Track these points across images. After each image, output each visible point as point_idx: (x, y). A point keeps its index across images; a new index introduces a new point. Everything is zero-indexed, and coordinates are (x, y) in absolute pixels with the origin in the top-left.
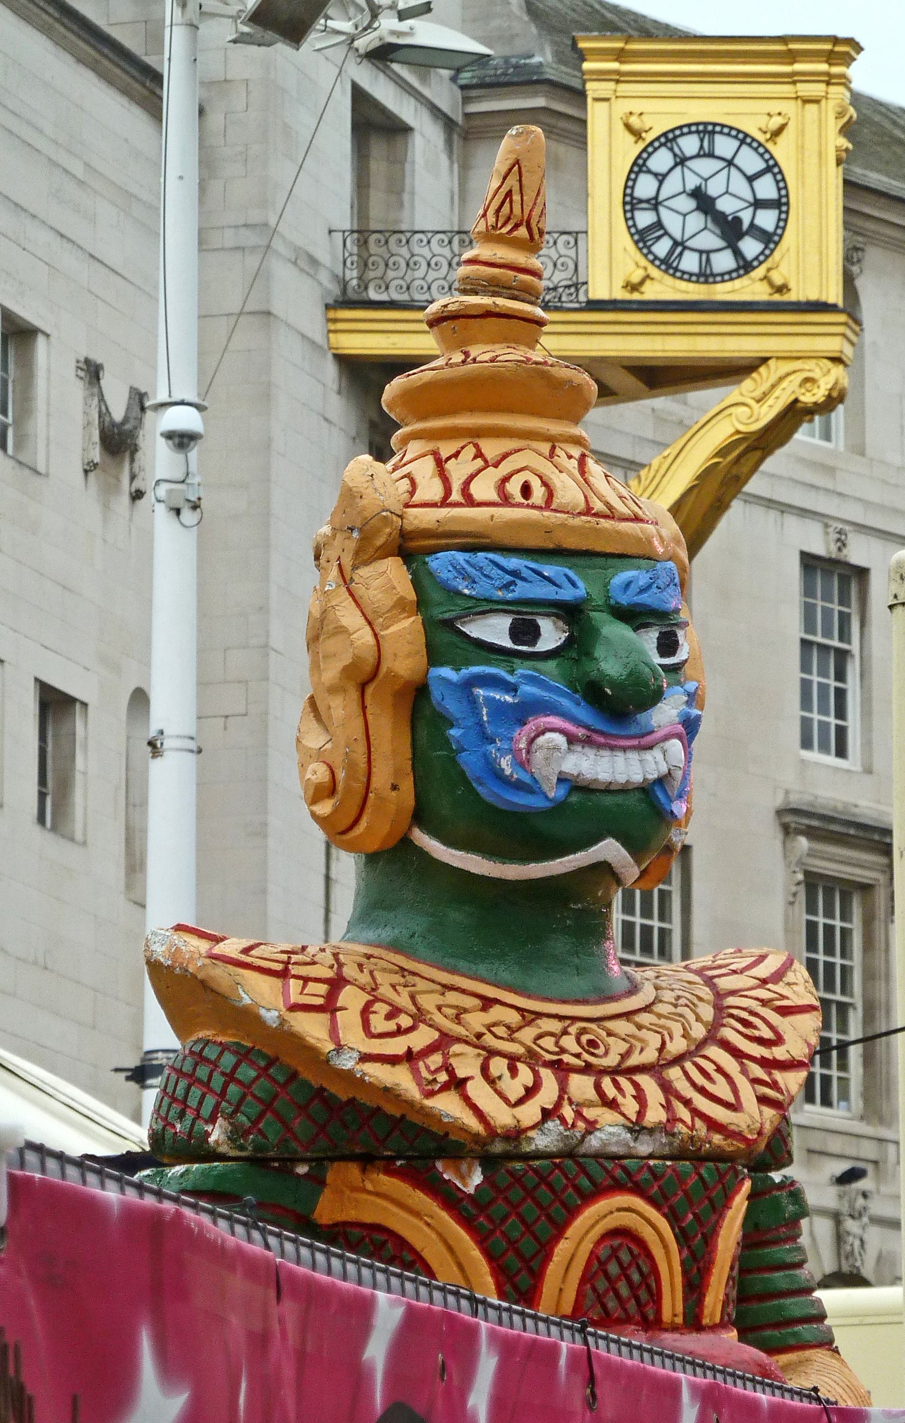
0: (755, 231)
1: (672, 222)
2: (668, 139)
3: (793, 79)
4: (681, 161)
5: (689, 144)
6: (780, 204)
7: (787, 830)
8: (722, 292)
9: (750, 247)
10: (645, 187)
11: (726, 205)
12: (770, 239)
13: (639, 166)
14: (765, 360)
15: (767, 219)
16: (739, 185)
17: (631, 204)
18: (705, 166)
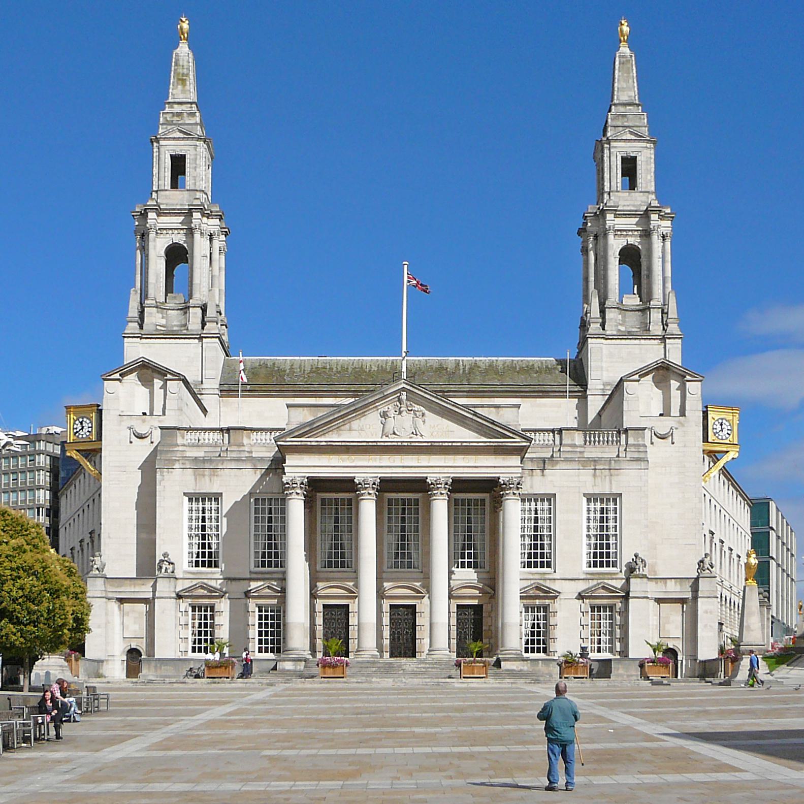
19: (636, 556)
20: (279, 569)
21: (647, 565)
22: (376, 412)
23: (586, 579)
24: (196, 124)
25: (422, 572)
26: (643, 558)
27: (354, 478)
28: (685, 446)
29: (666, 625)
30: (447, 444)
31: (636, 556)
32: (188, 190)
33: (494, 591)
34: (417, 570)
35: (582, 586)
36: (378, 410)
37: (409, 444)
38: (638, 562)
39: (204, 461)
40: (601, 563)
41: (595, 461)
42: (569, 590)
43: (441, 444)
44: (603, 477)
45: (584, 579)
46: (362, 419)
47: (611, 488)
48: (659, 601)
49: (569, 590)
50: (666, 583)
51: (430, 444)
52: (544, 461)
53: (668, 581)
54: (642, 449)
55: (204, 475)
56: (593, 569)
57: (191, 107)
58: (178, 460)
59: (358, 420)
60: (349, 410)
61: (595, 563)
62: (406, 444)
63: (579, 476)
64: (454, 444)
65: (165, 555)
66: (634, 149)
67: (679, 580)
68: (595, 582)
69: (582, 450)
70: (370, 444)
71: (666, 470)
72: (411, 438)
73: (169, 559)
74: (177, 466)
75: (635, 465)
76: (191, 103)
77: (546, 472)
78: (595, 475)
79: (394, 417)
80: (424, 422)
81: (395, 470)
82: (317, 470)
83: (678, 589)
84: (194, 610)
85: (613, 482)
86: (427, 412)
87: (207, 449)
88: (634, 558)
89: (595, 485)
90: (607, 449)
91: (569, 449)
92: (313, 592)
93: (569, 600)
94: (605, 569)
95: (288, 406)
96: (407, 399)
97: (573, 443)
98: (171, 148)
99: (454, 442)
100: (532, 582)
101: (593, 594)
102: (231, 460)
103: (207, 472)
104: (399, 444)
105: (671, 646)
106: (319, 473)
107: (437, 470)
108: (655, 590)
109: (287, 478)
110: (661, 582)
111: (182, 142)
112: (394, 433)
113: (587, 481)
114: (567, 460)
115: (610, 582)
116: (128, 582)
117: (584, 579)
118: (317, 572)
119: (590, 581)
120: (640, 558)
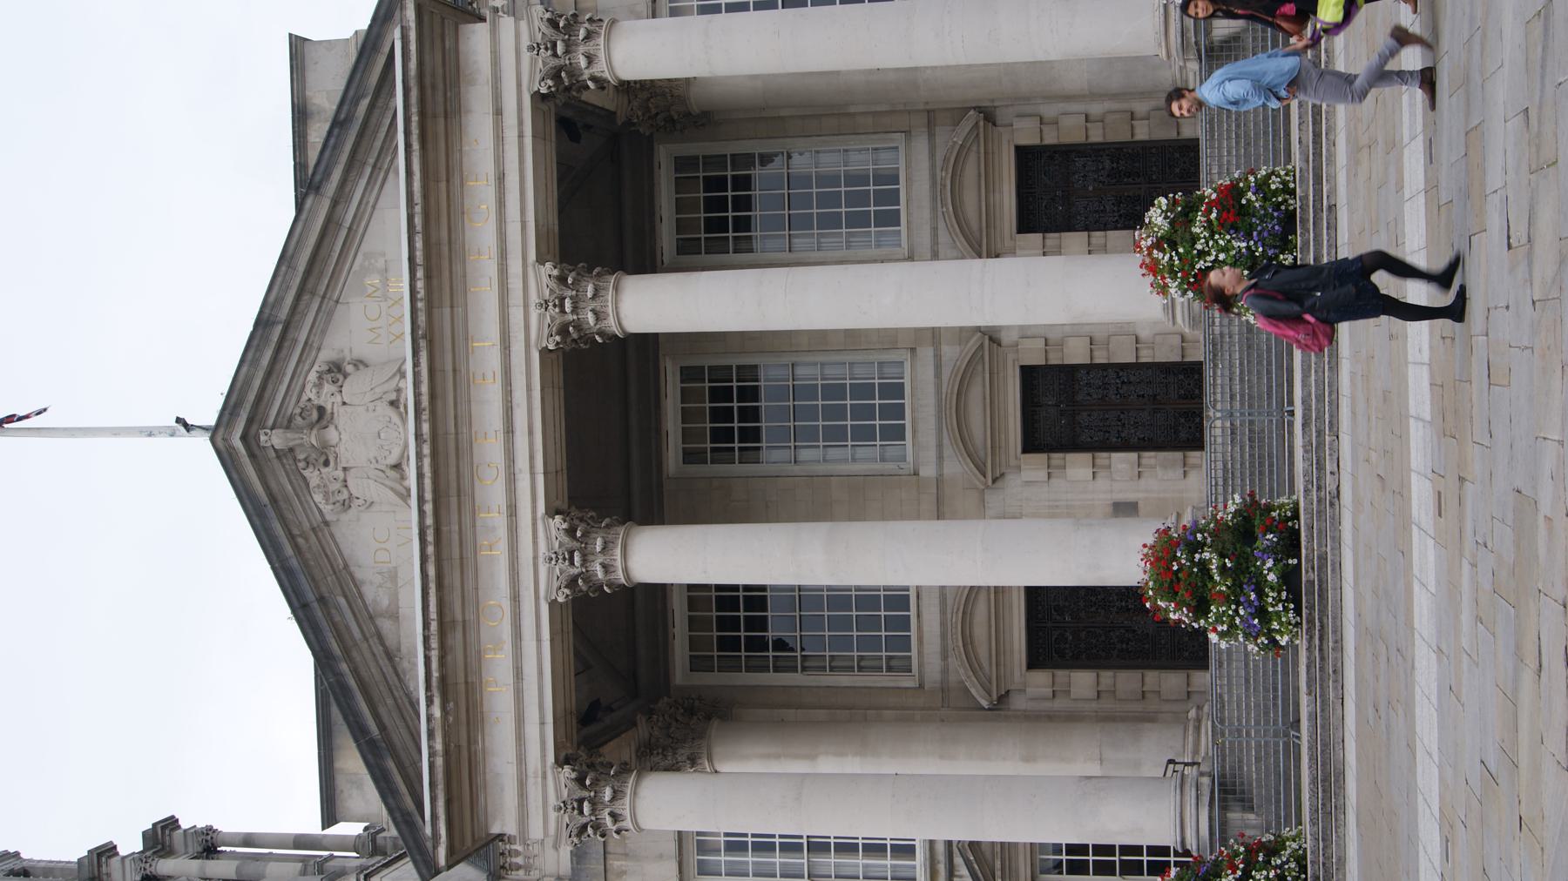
22: (334, 529)
25: (913, 350)
27: (553, 604)
30: (420, 285)
33: (969, 109)
34: (907, 365)
36: (327, 523)
37: (425, 416)
43: (420, 305)
46: (359, 575)
51: (423, 344)
62: (426, 427)
64: (419, 254)
70: (430, 549)
72: (406, 412)
79: (345, 469)
80: (359, 363)
82: (532, 731)
86: (326, 355)
92: (985, 703)
96: (288, 428)
99: (411, 259)
104: (426, 450)
106: (542, 723)
112: (397, 467)
118: (921, 686)
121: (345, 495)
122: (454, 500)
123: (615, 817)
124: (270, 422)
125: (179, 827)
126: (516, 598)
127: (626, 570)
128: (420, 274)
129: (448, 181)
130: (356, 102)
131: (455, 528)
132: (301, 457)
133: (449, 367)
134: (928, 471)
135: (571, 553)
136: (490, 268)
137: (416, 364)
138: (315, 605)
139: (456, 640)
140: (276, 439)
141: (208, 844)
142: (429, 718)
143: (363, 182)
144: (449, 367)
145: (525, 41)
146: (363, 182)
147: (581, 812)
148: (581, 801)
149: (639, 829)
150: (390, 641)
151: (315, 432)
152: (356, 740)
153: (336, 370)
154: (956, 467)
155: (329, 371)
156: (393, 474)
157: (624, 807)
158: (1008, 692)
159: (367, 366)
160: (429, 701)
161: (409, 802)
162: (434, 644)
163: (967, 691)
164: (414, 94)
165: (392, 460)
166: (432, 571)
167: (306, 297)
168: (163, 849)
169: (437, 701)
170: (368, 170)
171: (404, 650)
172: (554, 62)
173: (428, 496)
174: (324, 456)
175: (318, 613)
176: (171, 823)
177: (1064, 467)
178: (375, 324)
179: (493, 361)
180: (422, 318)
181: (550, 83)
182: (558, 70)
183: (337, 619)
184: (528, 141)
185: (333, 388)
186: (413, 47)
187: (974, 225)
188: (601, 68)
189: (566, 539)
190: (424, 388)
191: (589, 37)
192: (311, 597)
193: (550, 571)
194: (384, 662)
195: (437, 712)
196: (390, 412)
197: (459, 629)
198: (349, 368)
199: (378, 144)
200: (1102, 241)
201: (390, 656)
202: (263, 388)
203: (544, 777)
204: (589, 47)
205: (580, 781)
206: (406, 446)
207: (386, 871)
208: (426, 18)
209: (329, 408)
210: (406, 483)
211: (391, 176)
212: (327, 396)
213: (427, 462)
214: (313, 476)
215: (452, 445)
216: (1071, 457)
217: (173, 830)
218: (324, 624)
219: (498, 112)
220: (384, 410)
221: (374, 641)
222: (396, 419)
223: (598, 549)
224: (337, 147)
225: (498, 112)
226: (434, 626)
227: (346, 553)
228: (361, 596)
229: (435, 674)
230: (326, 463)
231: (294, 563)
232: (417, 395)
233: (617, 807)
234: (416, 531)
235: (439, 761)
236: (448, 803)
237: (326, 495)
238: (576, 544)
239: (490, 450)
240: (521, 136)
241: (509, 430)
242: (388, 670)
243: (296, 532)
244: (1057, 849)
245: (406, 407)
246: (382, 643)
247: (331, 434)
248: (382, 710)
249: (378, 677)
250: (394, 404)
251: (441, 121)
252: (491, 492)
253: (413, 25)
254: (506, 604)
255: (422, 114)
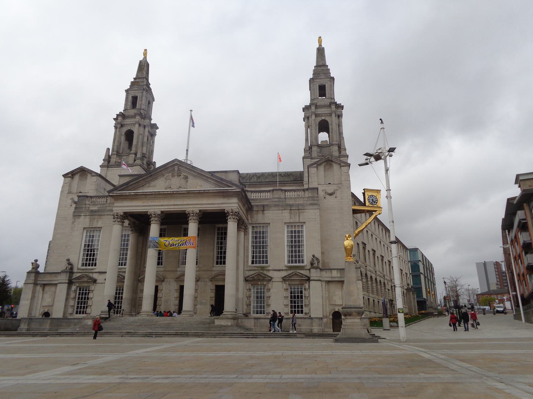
0: (376, 202)
1: (371, 201)
2: (370, 196)
3: (378, 192)
4: (371, 197)
5: (371, 196)
6: (377, 200)
7: (362, 244)
8: (374, 206)
9: (376, 203)
10: (369, 199)
11: (374, 200)
12: (377, 203)
13: (368, 197)
14: (377, 211)
15: (376, 201)
16: (375, 199)
17: (368, 200)
18: (373, 198)
19: (314, 256)
20: (123, 266)
21: (321, 262)
22: (163, 177)
23: (287, 270)
24: (144, 85)
26: (318, 257)
28: (342, 199)
29: (333, 297)
30: (196, 192)
31: (314, 256)
32: (137, 109)
35: (284, 274)
36: (164, 176)
37: (177, 192)
38: (314, 260)
39: (96, 211)
40: (296, 261)
41: (291, 206)
42: (277, 276)
44: (295, 214)
45: (285, 270)
47: (299, 220)
48: (328, 282)
49: (277, 276)
50: (331, 272)
51: (187, 192)
52: (264, 206)
53: (333, 271)
54: (316, 199)
55: (94, 219)
56: (291, 264)
57: (144, 79)
58: (83, 212)
59: (153, 182)
60: (147, 176)
61: (292, 261)
62: (175, 192)
63: (282, 213)
65: (68, 260)
66: (325, 82)
67: (339, 270)
68: (292, 271)
69: (284, 200)
70: (156, 193)
71: (332, 211)
72: (178, 189)
73: (70, 262)
74: (82, 215)
75: (311, 207)
76: (143, 78)
77: (265, 212)
78: (290, 213)
79: (171, 179)
80: (187, 181)
81: (170, 207)
83: (339, 275)
84: (80, 290)
85: (300, 216)
87: (99, 206)
88: (313, 258)
89: (291, 218)
90: (298, 199)
91: (277, 200)
93: (277, 282)
94: (298, 264)
95: (120, 176)
96: (179, 170)
97: (280, 197)
98: (133, 93)
99: (200, 190)
100: (257, 271)
101: (290, 279)
102: (108, 211)
103: (96, 217)
104: (172, 192)
105: (337, 310)
107: (192, 206)
108: (326, 275)
109: (113, 213)
110: (328, 272)
111: (137, 91)
112: (170, 187)
113: (286, 215)
114: (276, 206)
115: (300, 271)
116: (48, 275)
117: (285, 270)
119: (289, 271)
120: (316, 257)
121: (167, 179)
122: (165, 196)
123: (115, 221)
124: (179, 167)
125: (157, 129)
126: (149, 206)
127: (152, 223)
128: (198, 192)
129: (213, 196)
130: (225, 182)
131: (160, 197)
132: (173, 172)
133: (185, 196)
134: (179, 269)
135: (155, 215)
136: (199, 203)
137: (184, 191)
138: (150, 175)
139: (144, 196)
140: (176, 168)
141: (153, 135)
142: (131, 193)
143: (214, 182)
144: (185, 196)
145: (232, 208)
146: (214, 182)
147: (116, 216)
148: (118, 216)
149: (114, 224)
150: (145, 186)
151: (177, 175)
152: (129, 181)
153: (186, 178)
154: (179, 273)
155: (186, 177)
156: (169, 186)
157: (116, 223)
158: (141, 282)
159: (187, 182)
160: (134, 193)
161: (120, 189)
162: (142, 193)
163: (142, 275)
164: (225, 191)
165: (172, 187)
166: (153, 193)
167: (197, 173)
168: (152, 127)
169: (134, 194)
170: (215, 183)
171: (144, 188)
172: (230, 213)
173: (165, 193)
174: (173, 176)
175: (150, 175)
176: (157, 128)
177: (177, 292)
178: (193, 184)
179: (185, 203)
180: (191, 192)
181: (226, 212)
182: (229, 213)
183: (149, 178)
184: (218, 208)
185: (183, 178)
186: (232, 191)
187: (217, 278)
188: (229, 220)
189: (157, 214)
190: (181, 192)
191: (233, 218)
192: (152, 174)
193: (152, 211)
194: (142, 185)
195: (132, 194)
196: (179, 186)
197: (145, 197)
198: (186, 180)
199: (219, 184)
200: (213, 299)
201: (143, 186)
202: (184, 166)
203: (122, 210)
204: (232, 218)
205: (121, 216)
206: (173, 189)
207: (141, 168)
208: (237, 192)
209: (181, 177)
210: (168, 189)
211: (215, 186)
212: (182, 176)
213: (169, 192)
214: (170, 174)
215: (173, 196)
216: (178, 293)
217: (156, 128)
218: (147, 176)
219: (223, 204)
220: (179, 185)
221: (145, 183)
222: (178, 187)
223: (155, 219)
224: (218, 178)
225: (223, 204)
226: (145, 193)
227: (160, 179)
228: (152, 181)
229: (138, 194)
230: (172, 176)
231: (157, 171)
232: (180, 191)
233: (116, 222)
234: (160, 191)
235: (125, 194)
236: (119, 195)
237: (167, 176)
238: (156, 215)
239: (172, 202)
240: (219, 207)
241: (174, 205)
242: (140, 186)
243: (162, 171)
244: (123, 290)
245: (180, 189)
246: (145, 185)
247: (176, 177)
248: (134, 185)
249: (140, 184)
250: (180, 187)
251: (222, 195)
252: (165, 202)
253: (236, 191)
254: (149, 204)
255: (222, 192)
